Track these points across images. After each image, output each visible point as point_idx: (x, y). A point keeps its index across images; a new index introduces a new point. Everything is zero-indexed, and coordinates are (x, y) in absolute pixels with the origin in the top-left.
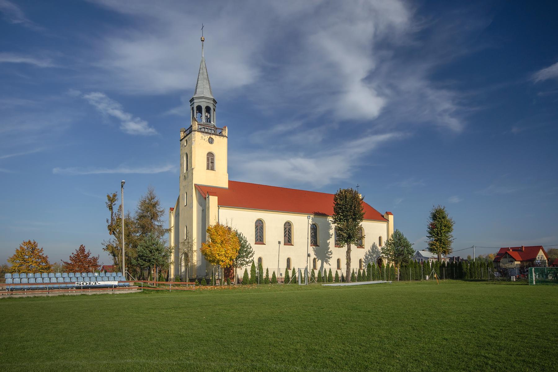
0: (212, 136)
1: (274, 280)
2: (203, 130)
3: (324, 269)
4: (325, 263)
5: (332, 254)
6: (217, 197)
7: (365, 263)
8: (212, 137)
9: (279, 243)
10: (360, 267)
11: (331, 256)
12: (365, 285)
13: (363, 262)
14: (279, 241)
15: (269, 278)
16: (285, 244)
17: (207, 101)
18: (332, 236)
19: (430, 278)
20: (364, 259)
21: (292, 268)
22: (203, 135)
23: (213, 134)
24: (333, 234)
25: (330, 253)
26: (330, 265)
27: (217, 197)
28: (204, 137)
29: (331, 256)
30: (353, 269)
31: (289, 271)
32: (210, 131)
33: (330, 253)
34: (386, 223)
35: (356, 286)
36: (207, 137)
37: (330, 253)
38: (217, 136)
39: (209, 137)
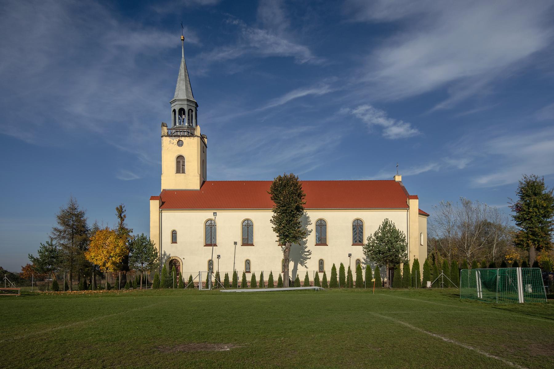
0: (181, 138)
1: (191, 284)
2: (175, 134)
3: (297, 274)
4: (299, 266)
5: (310, 254)
6: (158, 201)
7: (365, 264)
8: (180, 139)
9: (235, 243)
10: (246, 269)
11: (308, 257)
12: (279, 292)
13: (363, 263)
14: (236, 241)
15: (257, 281)
16: (244, 244)
17: (180, 103)
18: (310, 232)
19: (432, 286)
20: (364, 260)
21: (215, 271)
22: (171, 140)
23: (182, 136)
24: (312, 230)
25: (307, 253)
26: (307, 268)
27: (158, 201)
28: (173, 141)
29: (308, 257)
30: (307, 272)
31: (247, 275)
32: (179, 134)
33: (308, 252)
34: (406, 210)
35: (259, 292)
36: (176, 140)
37: (307, 253)
38: (186, 138)
39: (177, 140)
